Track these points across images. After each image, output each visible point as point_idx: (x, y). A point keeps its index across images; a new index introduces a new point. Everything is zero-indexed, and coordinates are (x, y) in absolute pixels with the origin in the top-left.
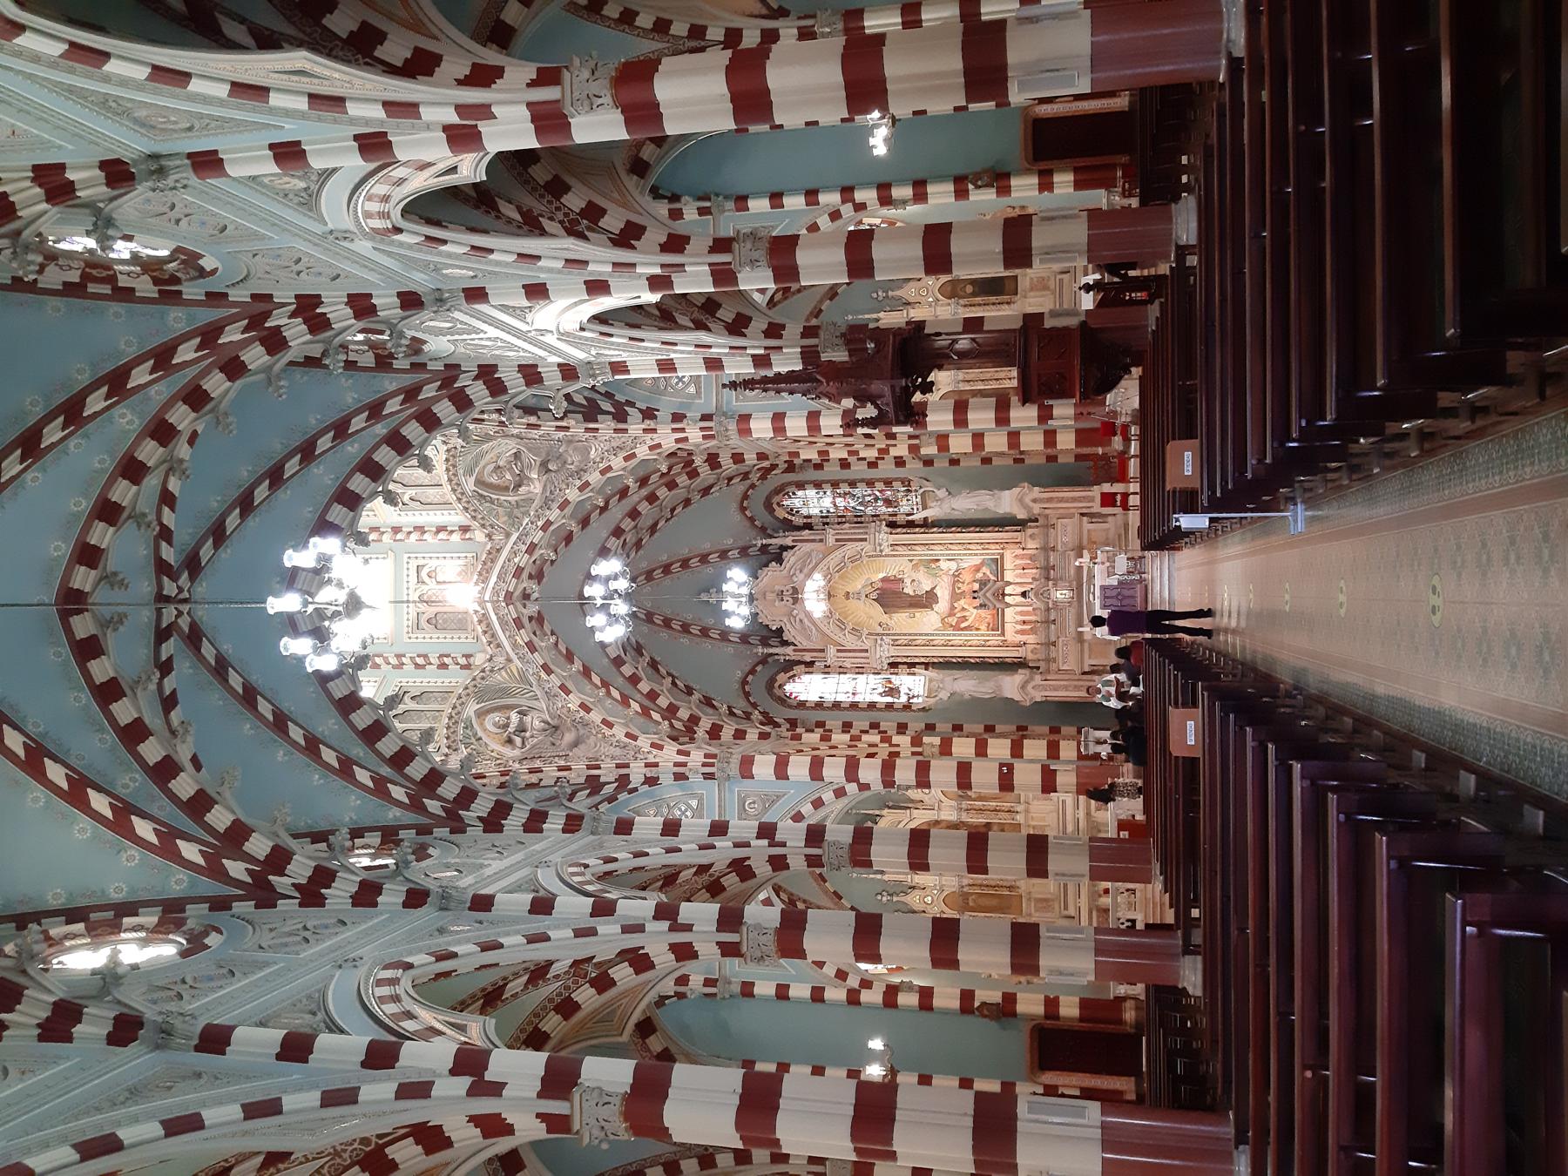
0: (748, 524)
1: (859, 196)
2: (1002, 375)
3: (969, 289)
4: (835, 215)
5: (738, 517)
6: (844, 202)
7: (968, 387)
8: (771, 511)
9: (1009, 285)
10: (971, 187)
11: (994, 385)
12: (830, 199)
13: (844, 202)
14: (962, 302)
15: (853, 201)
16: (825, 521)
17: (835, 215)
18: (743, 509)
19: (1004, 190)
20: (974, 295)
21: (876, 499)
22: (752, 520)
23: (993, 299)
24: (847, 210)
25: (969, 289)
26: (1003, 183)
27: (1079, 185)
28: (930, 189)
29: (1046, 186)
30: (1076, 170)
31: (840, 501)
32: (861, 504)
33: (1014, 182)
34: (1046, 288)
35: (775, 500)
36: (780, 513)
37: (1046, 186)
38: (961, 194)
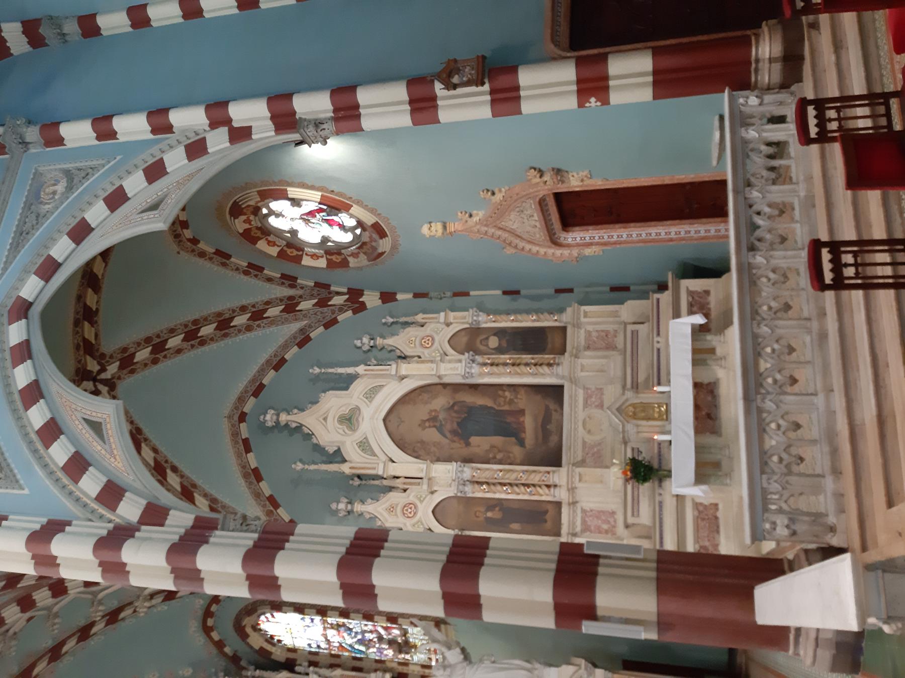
0: (214, 651)
1: (239, 113)
2: (535, 479)
3: (494, 342)
4: (196, 149)
5: (200, 639)
6: (214, 125)
7: (480, 493)
8: (244, 636)
9: (554, 340)
10: (438, 87)
11: (523, 495)
12: (189, 119)
13: (214, 125)
14: (479, 359)
15: (228, 121)
16: (314, 659)
17: (196, 149)
18: (207, 630)
19: (506, 99)
20: (500, 350)
21: (380, 639)
22: (220, 645)
23: (527, 358)
24: (218, 140)
25: (494, 342)
26: (503, 81)
27: (666, 83)
28: (364, 96)
29: (593, 85)
30: (657, 53)
31: (331, 633)
32: (360, 642)
33: (527, 77)
34: (611, 347)
35: (247, 621)
36: (256, 642)
37: (593, 85)
38: (423, 106)
